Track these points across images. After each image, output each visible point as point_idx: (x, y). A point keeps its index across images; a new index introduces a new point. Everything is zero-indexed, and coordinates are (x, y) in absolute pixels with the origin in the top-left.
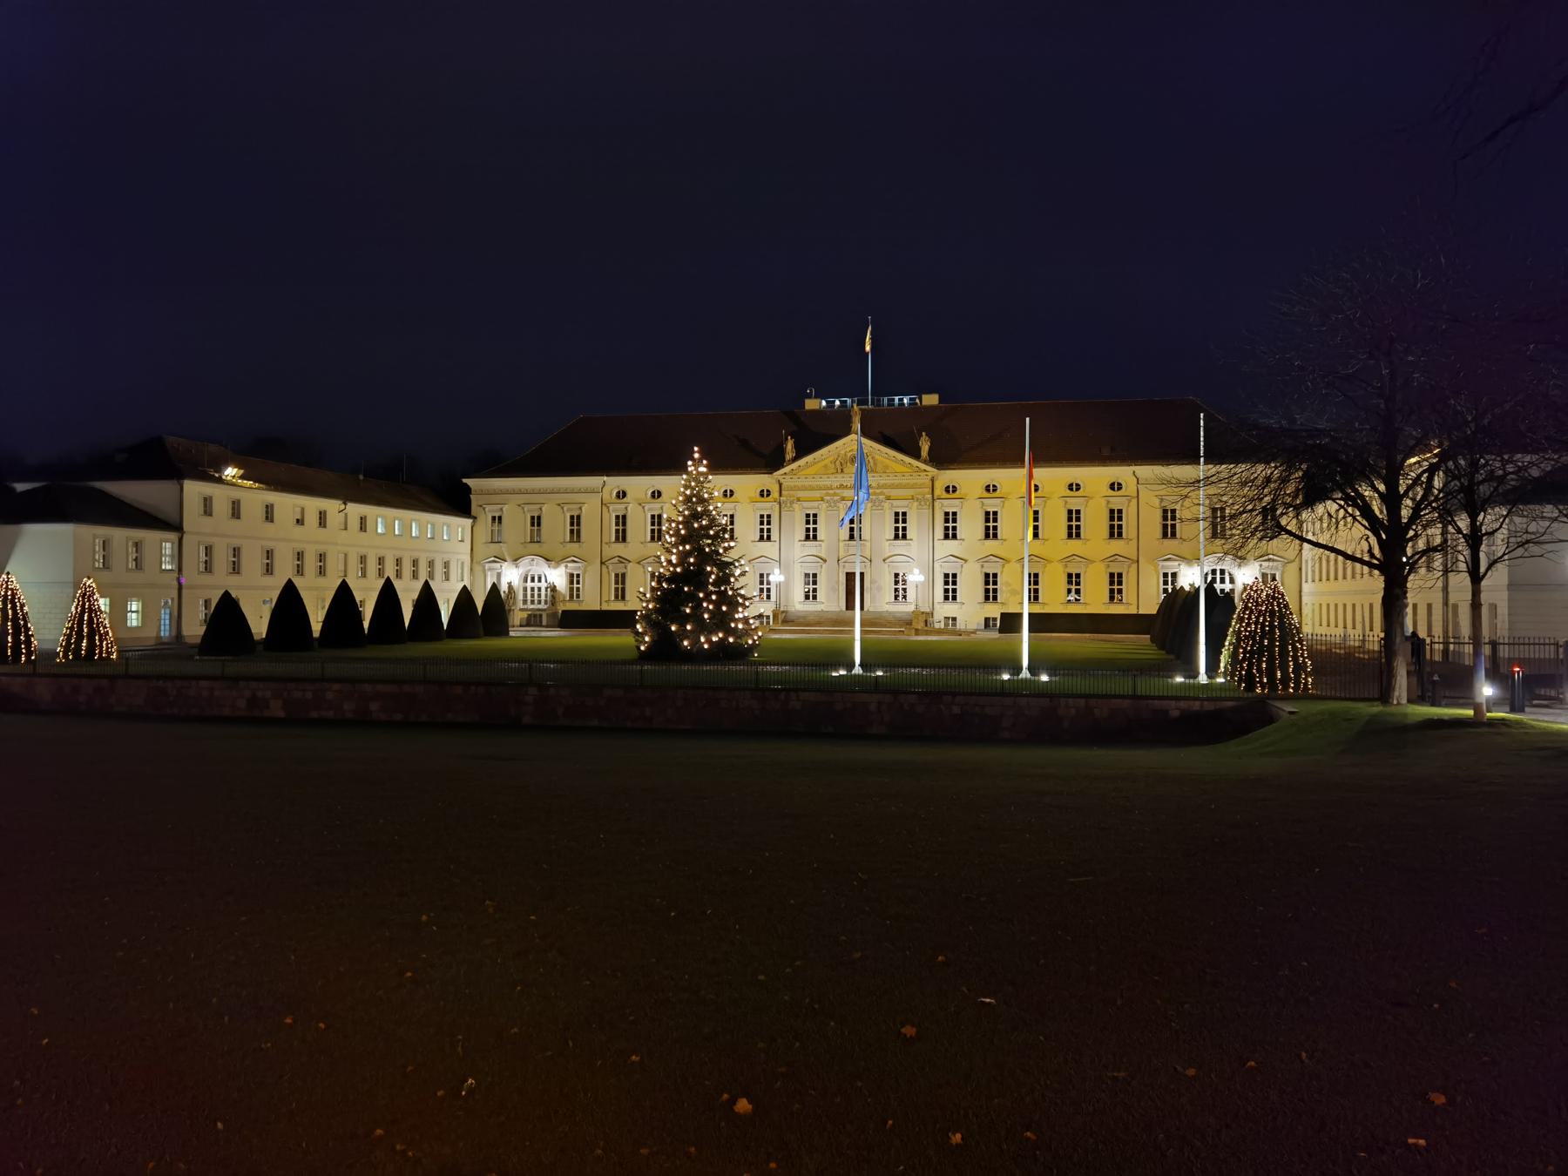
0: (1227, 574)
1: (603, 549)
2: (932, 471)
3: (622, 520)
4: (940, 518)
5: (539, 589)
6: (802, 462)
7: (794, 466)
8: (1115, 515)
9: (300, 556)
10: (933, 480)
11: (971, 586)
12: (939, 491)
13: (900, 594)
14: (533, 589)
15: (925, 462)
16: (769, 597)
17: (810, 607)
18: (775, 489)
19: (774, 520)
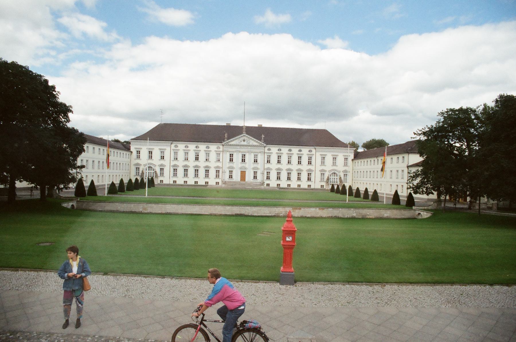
0: (336, 175)
1: (171, 162)
2: (265, 145)
3: (176, 153)
4: (266, 157)
5: (151, 173)
6: (230, 140)
7: (228, 141)
8: (310, 159)
9: (99, 162)
10: (265, 147)
11: (273, 175)
12: (266, 151)
13: (255, 177)
14: (149, 173)
15: (264, 143)
16: (219, 177)
17: (231, 180)
18: (221, 147)
19: (221, 155)
